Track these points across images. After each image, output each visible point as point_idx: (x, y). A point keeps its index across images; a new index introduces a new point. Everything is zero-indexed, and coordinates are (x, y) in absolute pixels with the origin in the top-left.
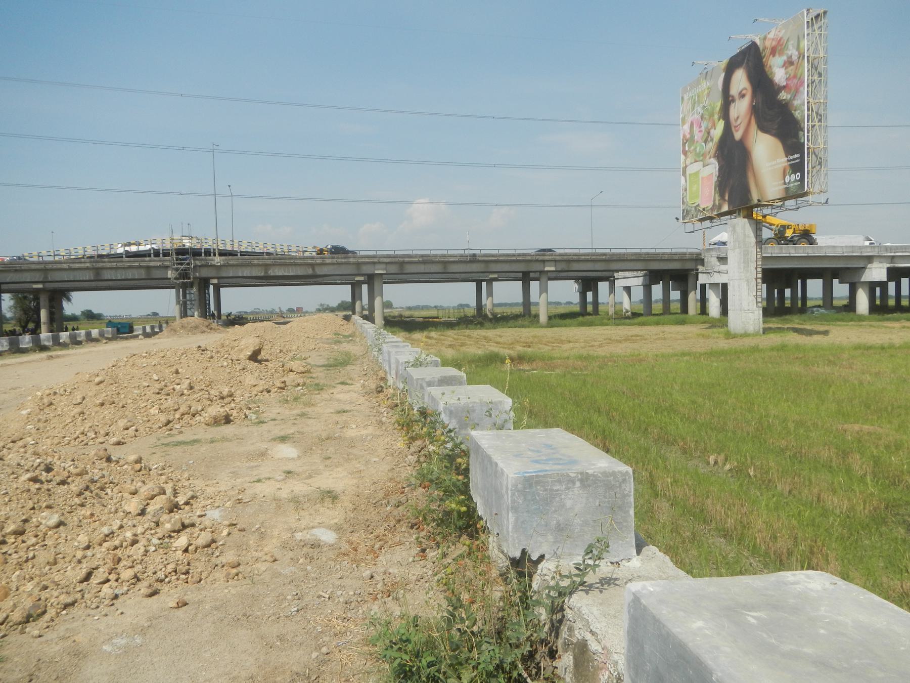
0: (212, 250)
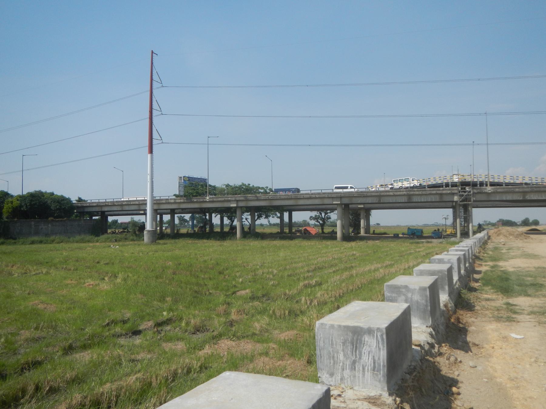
0: (485, 183)
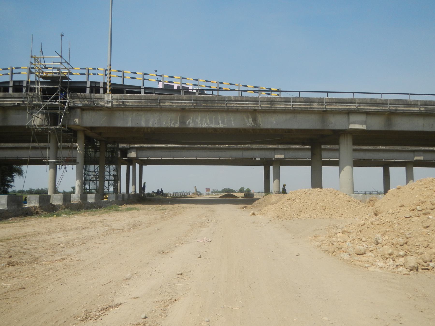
0: (102, 85)
